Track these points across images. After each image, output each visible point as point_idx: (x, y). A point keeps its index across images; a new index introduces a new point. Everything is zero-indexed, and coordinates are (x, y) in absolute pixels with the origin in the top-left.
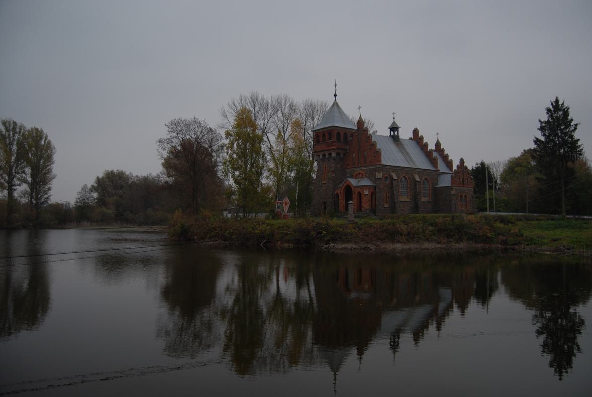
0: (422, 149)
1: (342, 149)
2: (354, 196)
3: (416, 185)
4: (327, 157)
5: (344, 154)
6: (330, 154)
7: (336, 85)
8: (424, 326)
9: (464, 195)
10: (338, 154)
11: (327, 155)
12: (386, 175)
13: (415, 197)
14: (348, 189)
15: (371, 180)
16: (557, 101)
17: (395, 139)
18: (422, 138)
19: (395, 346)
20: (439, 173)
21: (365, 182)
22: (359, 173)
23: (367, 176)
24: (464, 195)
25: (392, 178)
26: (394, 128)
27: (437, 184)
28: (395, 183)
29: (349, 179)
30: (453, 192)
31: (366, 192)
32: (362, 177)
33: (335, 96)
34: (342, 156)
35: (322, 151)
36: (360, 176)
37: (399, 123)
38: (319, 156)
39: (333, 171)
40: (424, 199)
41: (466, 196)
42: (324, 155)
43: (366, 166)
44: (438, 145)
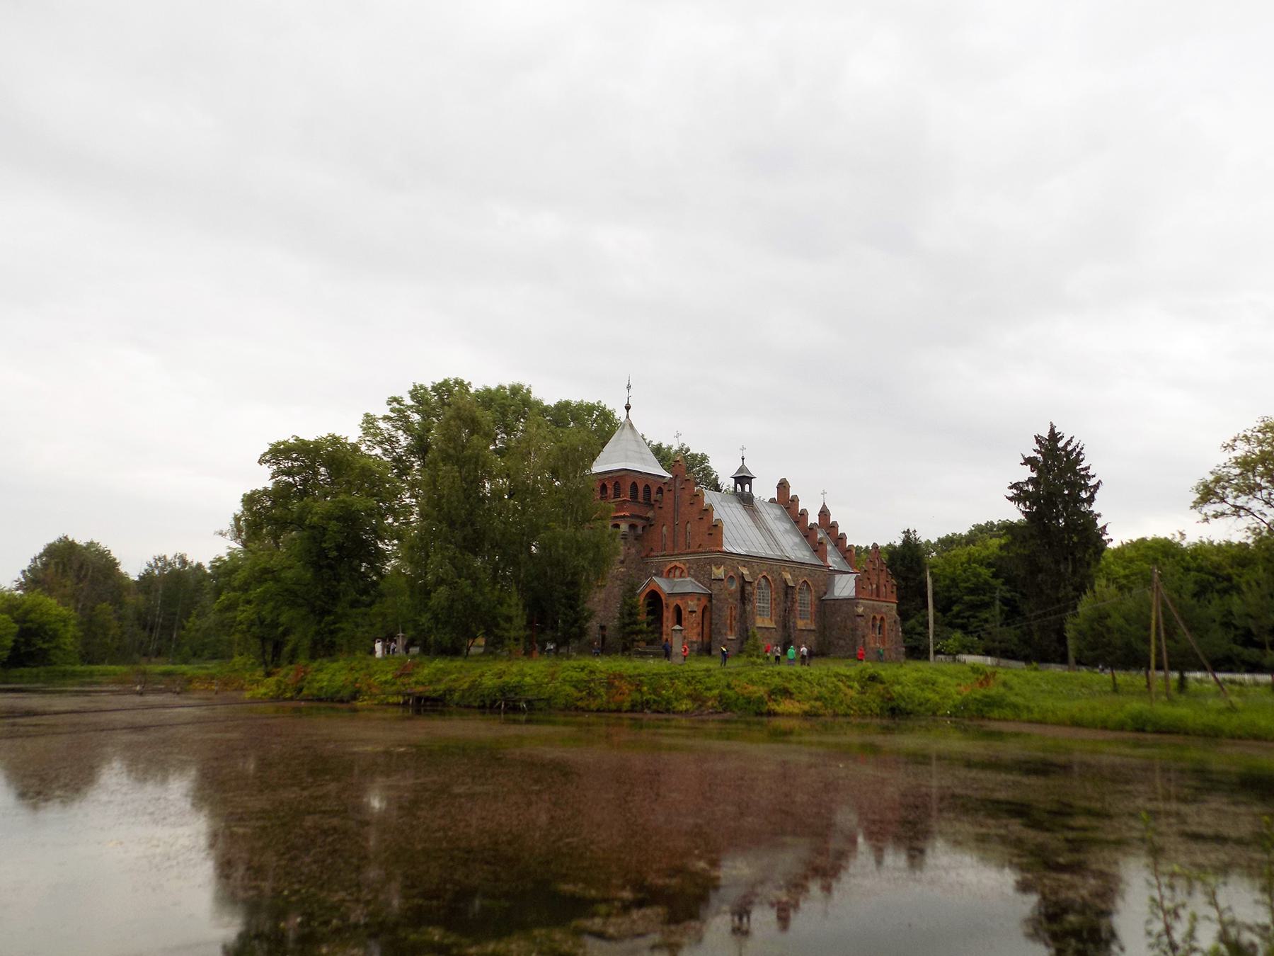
0: (797, 522)
1: (641, 517)
2: (665, 614)
6: (617, 526)
7: (629, 387)
8: (797, 886)
9: (878, 617)
10: (632, 527)
13: (785, 623)
14: (655, 599)
16: (1054, 436)
17: (746, 500)
18: (795, 500)
19: (740, 932)
21: (688, 585)
22: (676, 567)
23: (692, 572)
24: (878, 617)
25: (742, 576)
28: (749, 588)
31: (692, 604)
33: (628, 408)
34: (639, 531)
36: (678, 573)
37: (753, 469)
39: (622, 562)
40: (801, 624)
41: (882, 619)
44: (824, 513)
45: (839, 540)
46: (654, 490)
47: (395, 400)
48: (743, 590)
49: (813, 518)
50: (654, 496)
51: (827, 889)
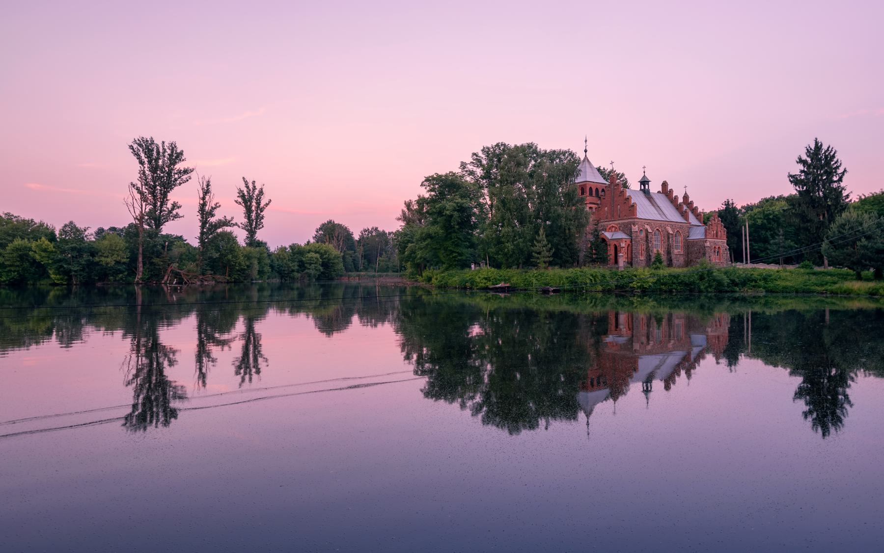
3: (669, 238)
8: (675, 372)
10: (590, 208)
16: (818, 147)
17: (646, 193)
18: (671, 191)
19: (647, 391)
20: (691, 226)
26: (644, 182)
30: (708, 244)
33: (586, 151)
37: (649, 178)
40: (676, 251)
44: (686, 197)
45: (694, 210)
46: (600, 190)
47: (474, 154)
48: (647, 237)
49: (680, 200)
50: (600, 193)
51: (689, 375)
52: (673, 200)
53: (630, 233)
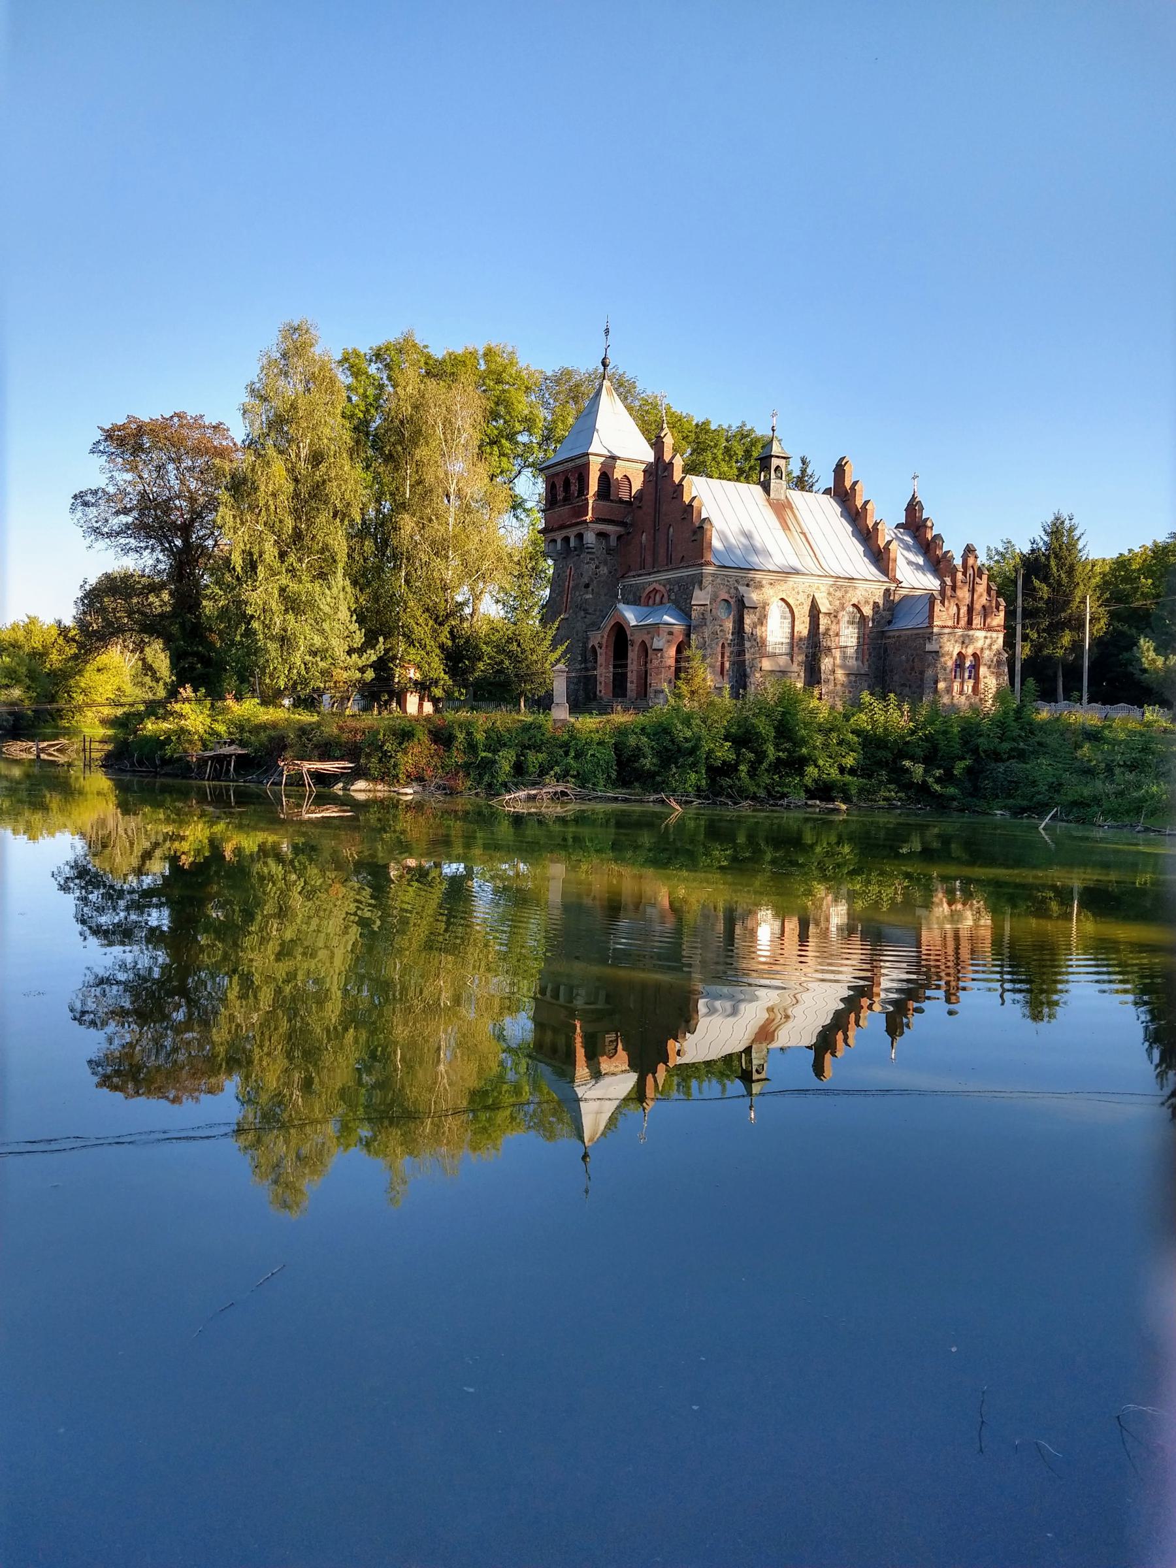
4: (572, 544)
5: (619, 538)
6: (580, 536)
7: (607, 331)
10: (601, 535)
11: (559, 541)
12: (726, 597)
15: (681, 609)
22: (655, 591)
27: (890, 622)
29: (621, 606)
32: (661, 603)
34: (613, 541)
35: (562, 527)
38: (554, 541)
39: (587, 586)
42: (566, 540)
43: (672, 569)
52: (855, 515)
53: (684, 611)
